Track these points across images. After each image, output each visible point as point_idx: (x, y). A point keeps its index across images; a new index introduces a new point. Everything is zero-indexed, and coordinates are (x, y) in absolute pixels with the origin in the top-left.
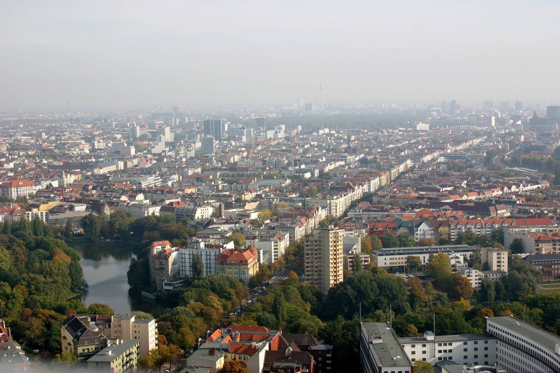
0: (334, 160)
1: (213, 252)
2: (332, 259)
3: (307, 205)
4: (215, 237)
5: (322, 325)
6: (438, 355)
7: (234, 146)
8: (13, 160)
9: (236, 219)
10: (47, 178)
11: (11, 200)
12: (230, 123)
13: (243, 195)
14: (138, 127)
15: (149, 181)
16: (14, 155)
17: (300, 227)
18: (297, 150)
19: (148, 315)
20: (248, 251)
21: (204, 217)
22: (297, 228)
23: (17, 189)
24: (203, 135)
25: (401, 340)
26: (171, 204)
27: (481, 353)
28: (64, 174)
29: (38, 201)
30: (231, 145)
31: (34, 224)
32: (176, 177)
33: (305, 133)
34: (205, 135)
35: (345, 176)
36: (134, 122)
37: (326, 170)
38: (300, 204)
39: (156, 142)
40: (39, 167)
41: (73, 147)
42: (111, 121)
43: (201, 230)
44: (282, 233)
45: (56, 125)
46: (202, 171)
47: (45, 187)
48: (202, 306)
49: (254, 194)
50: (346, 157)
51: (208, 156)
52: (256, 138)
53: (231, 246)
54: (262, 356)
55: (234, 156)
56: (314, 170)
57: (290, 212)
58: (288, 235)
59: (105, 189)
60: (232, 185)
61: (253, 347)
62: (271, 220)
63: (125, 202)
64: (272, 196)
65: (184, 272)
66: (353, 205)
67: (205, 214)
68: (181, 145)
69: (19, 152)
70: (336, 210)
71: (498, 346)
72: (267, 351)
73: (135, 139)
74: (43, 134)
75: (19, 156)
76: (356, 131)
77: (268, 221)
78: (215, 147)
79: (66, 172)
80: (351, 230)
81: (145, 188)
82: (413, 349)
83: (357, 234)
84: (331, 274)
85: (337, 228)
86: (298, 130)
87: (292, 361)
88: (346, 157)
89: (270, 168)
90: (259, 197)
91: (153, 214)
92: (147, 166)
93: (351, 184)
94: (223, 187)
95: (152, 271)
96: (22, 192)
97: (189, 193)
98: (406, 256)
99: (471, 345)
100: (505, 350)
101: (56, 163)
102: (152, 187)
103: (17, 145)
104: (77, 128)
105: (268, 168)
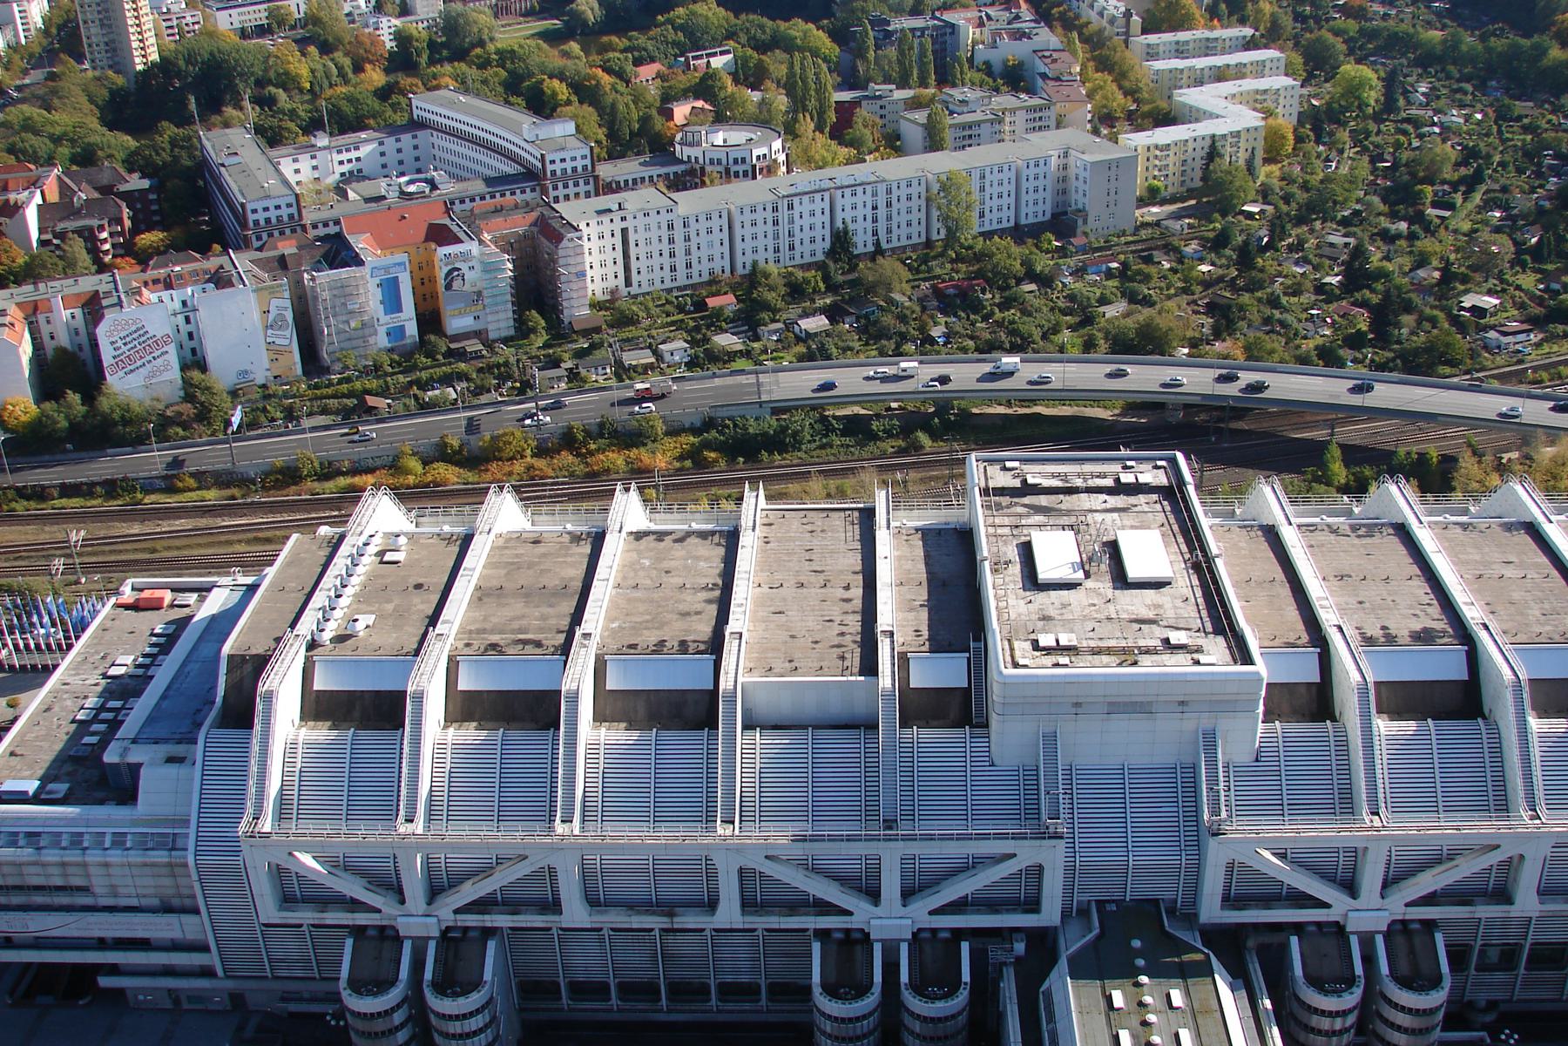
5: (130, 142)
6: (340, 169)
25: (273, 153)
27: (408, 154)
54: (31, 216)
61: (12, 203)
71: (437, 142)
72: (39, 206)
82: (297, 166)
84: (135, 53)
87: (90, 215)
98: (265, 6)
99: (390, 142)
100: (451, 146)
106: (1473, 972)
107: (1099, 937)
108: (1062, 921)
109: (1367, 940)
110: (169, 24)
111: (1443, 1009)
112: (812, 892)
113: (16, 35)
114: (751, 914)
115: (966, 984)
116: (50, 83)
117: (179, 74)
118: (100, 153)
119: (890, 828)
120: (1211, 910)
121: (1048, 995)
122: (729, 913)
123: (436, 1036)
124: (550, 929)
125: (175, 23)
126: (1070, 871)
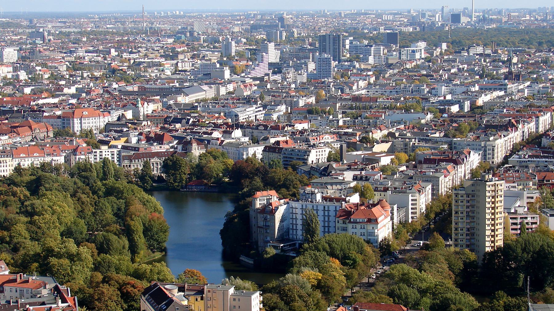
0: (490, 89)
1: (332, 206)
2: (489, 220)
3: (455, 148)
4: (334, 186)
7: (358, 70)
8: (75, 83)
9: (362, 164)
10: (117, 108)
11: (74, 135)
12: (352, 38)
13: (371, 134)
14: (233, 43)
15: (248, 113)
16: (77, 76)
17: (445, 177)
18: (441, 76)
19: (248, 284)
20: (379, 207)
21: (320, 161)
22: (442, 178)
23: (81, 120)
24: (318, 54)
26: (278, 143)
28: (140, 102)
29: (108, 136)
30: (354, 67)
31: (103, 167)
32: (283, 108)
33: (451, 53)
34: (320, 54)
35: (505, 110)
36: (228, 36)
37: (480, 102)
38: (446, 146)
39: (257, 62)
40: (109, 92)
41: (150, 67)
42: (199, 34)
43: (317, 178)
44: (423, 184)
45: (128, 39)
46: (317, 101)
47: (115, 119)
48: (320, 276)
49: (385, 132)
50: (506, 85)
51: (324, 82)
52: (387, 59)
53: (355, 199)
55: (357, 82)
56: (464, 102)
57: (432, 157)
58: (430, 186)
59: (193, 122)
60: (356, 120)
62: (407, 167)
63: (218, 139)
64: (409, 135)
65: (295, 231)
66: (515, 150)
67: (321, 157)
68: (288, 66)
69: (82, 73)
70: (493, 155)
73: (230, 58)
74: (113, 51)
75: (83, 78)
76: (518, 51)
77: (404, 168)
78: (334, 71)
79: (142, 99)
80: (514, 182)
81: (244, 122)
83: (521, 187)
84: (487, 239)
85: (497, 179)
86: (441, 49)
88: (506, 85)
89: (405, 98)
90: (391, 135)
91: (254, 155)
92: (245, 94)
93: (513, 121)
94: (344, 122)
95: (254, 229)
96: (87, 125)
97: (300, 129)
101: (130, 88)
102: (252, 121)
103: (80, 63)
104: (155, 43)
105: (402, 99)
110: (515, 221)
113: (407, 216)
116: (424, 251)
117: (515, 259)
118: (452, 306)
125: (519, 221)
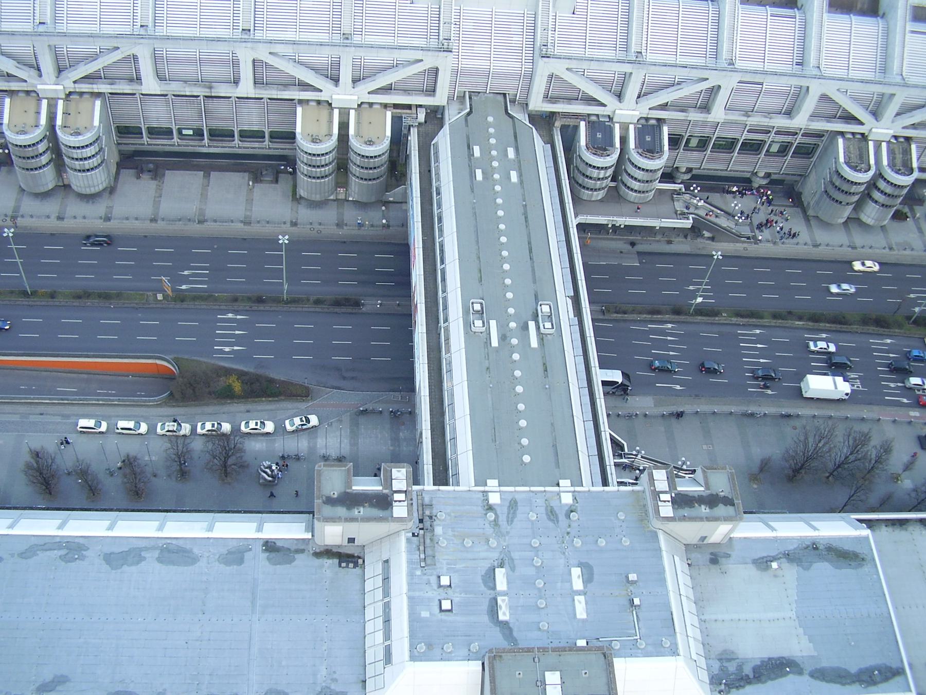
106: (681, 151)
107: (469, 114)
108: (448, 103)
109: (625, 128)
111: (662, 170)
112: (298, 77)
114: (260, 88)
115: (388, 137)
119: (347, 39)
120: (537, 104)
121: (436, 146)
122: (246, 88)
123: (65, 158)
124: (135, 94)
126: (456, 72)
